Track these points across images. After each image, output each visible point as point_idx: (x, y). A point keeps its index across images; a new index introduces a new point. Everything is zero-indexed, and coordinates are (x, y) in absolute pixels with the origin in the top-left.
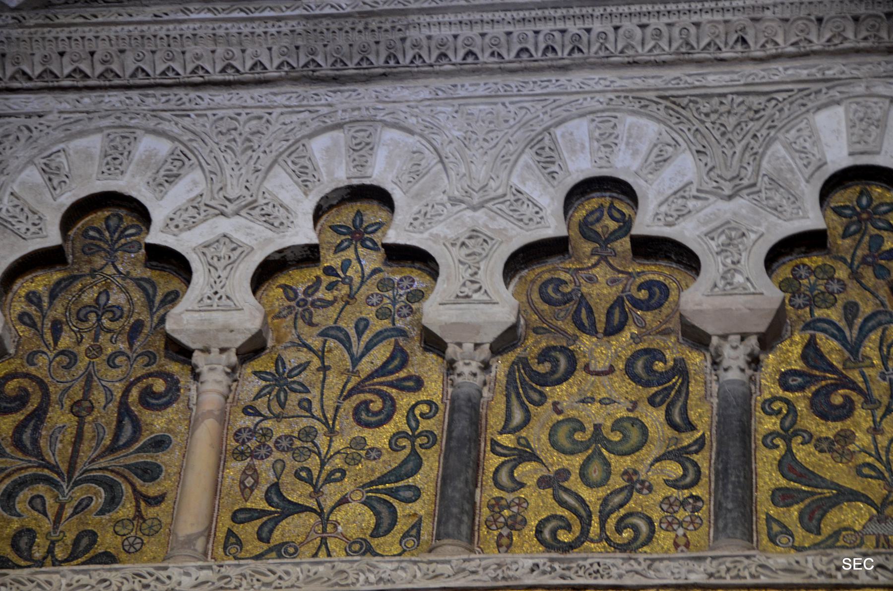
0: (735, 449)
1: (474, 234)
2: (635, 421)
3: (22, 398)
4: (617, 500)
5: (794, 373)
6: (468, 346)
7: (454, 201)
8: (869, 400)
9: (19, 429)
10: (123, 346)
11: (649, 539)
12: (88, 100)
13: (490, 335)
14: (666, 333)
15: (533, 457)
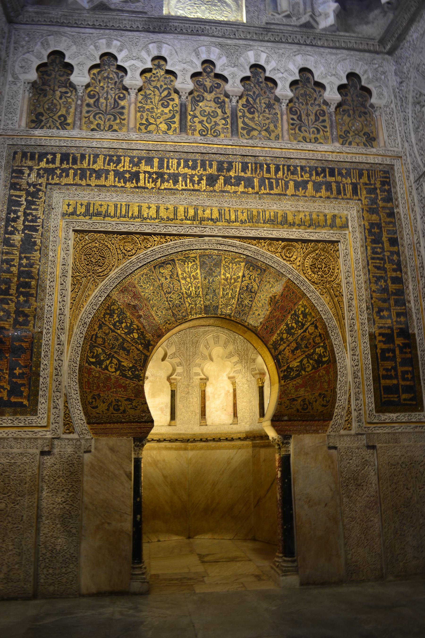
0: (235, 119)
1: (184, 69)
2: (216, 112)
3: (94, 96)
4: (213, 127)
5: (244, 104)
6: (184, 93)
7: (180, 61)
8: (258, 111)
9: (95, 102)
10: (113, 86)
11: (219, 135)
12: (102, 31)
13: (189, 91)
14: (221, 94)
15: (197, 117)
